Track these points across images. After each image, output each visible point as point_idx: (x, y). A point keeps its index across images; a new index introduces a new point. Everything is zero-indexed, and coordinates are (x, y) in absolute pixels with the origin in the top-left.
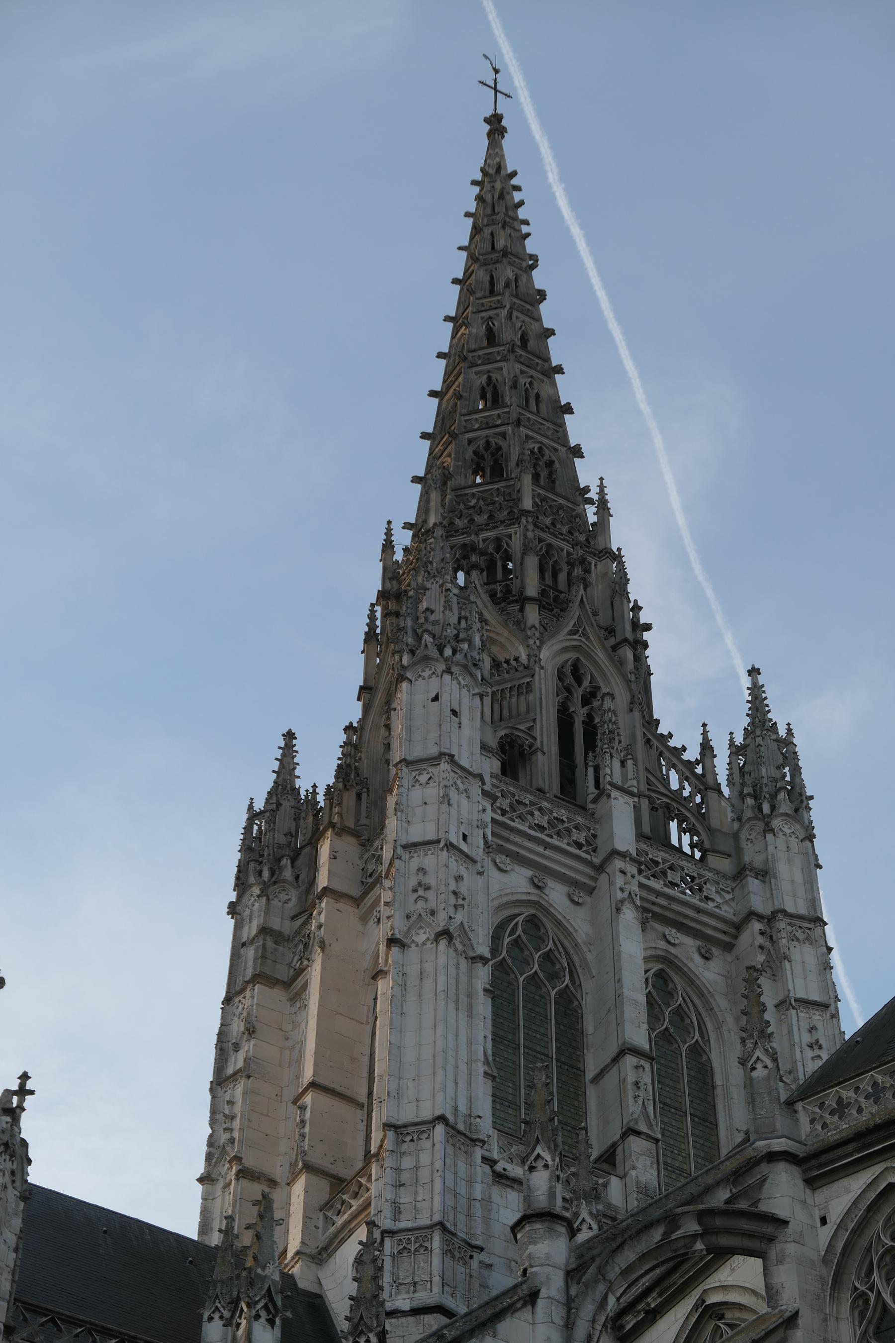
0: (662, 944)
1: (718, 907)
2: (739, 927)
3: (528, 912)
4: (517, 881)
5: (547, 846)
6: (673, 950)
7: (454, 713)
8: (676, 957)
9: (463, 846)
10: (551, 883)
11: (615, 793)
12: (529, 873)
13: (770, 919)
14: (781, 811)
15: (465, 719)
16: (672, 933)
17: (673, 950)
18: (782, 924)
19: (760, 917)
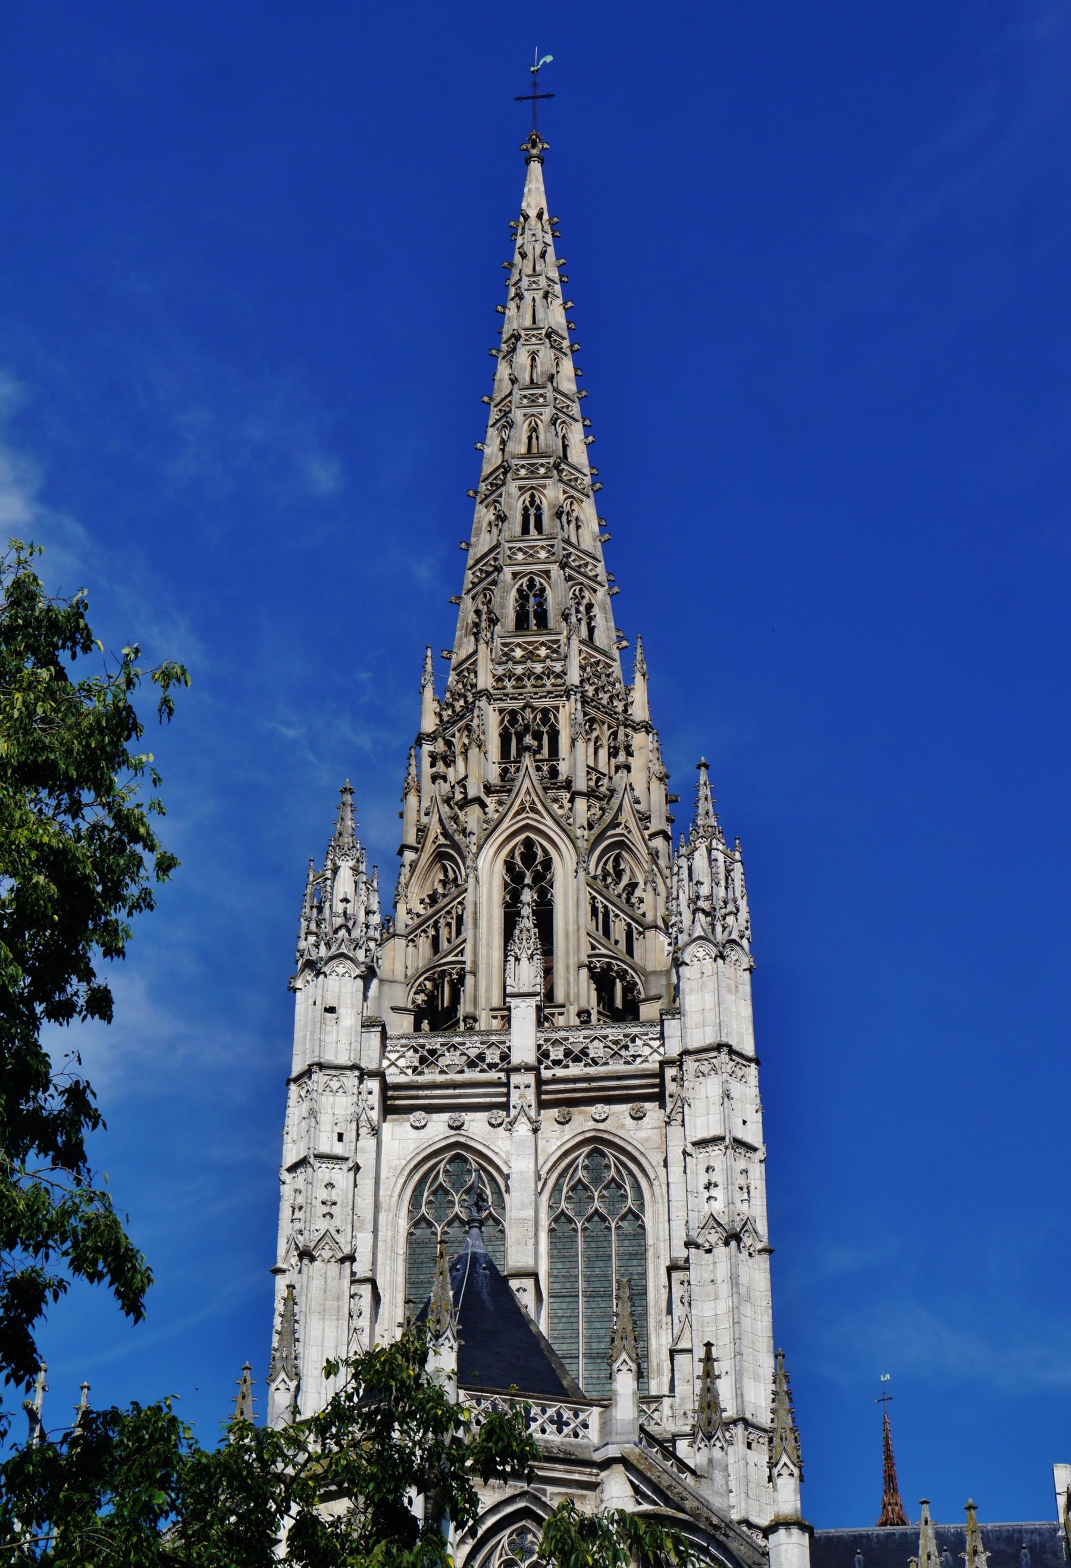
0: (592, 1124)
1: (646, 1061)
2: (661, 1075)
3: (448, 1155)
4: (438, 1128)
5: (455, 1085)
6: (601, 1126)
7: (331, 1010)
8: (605, 1131)
9: (338, 1149)
10: (467, 1117)
11: (513, 1002)
12: (445, 1116)
13: (678, 1062)
14: (696, 935)
15: (342, 1011)
16: (600, 1110)
17: (601, 1126)
18: (690, 1064)
19: (670, 1063)
